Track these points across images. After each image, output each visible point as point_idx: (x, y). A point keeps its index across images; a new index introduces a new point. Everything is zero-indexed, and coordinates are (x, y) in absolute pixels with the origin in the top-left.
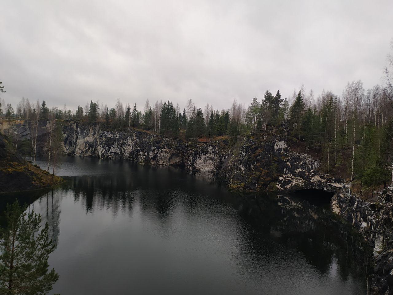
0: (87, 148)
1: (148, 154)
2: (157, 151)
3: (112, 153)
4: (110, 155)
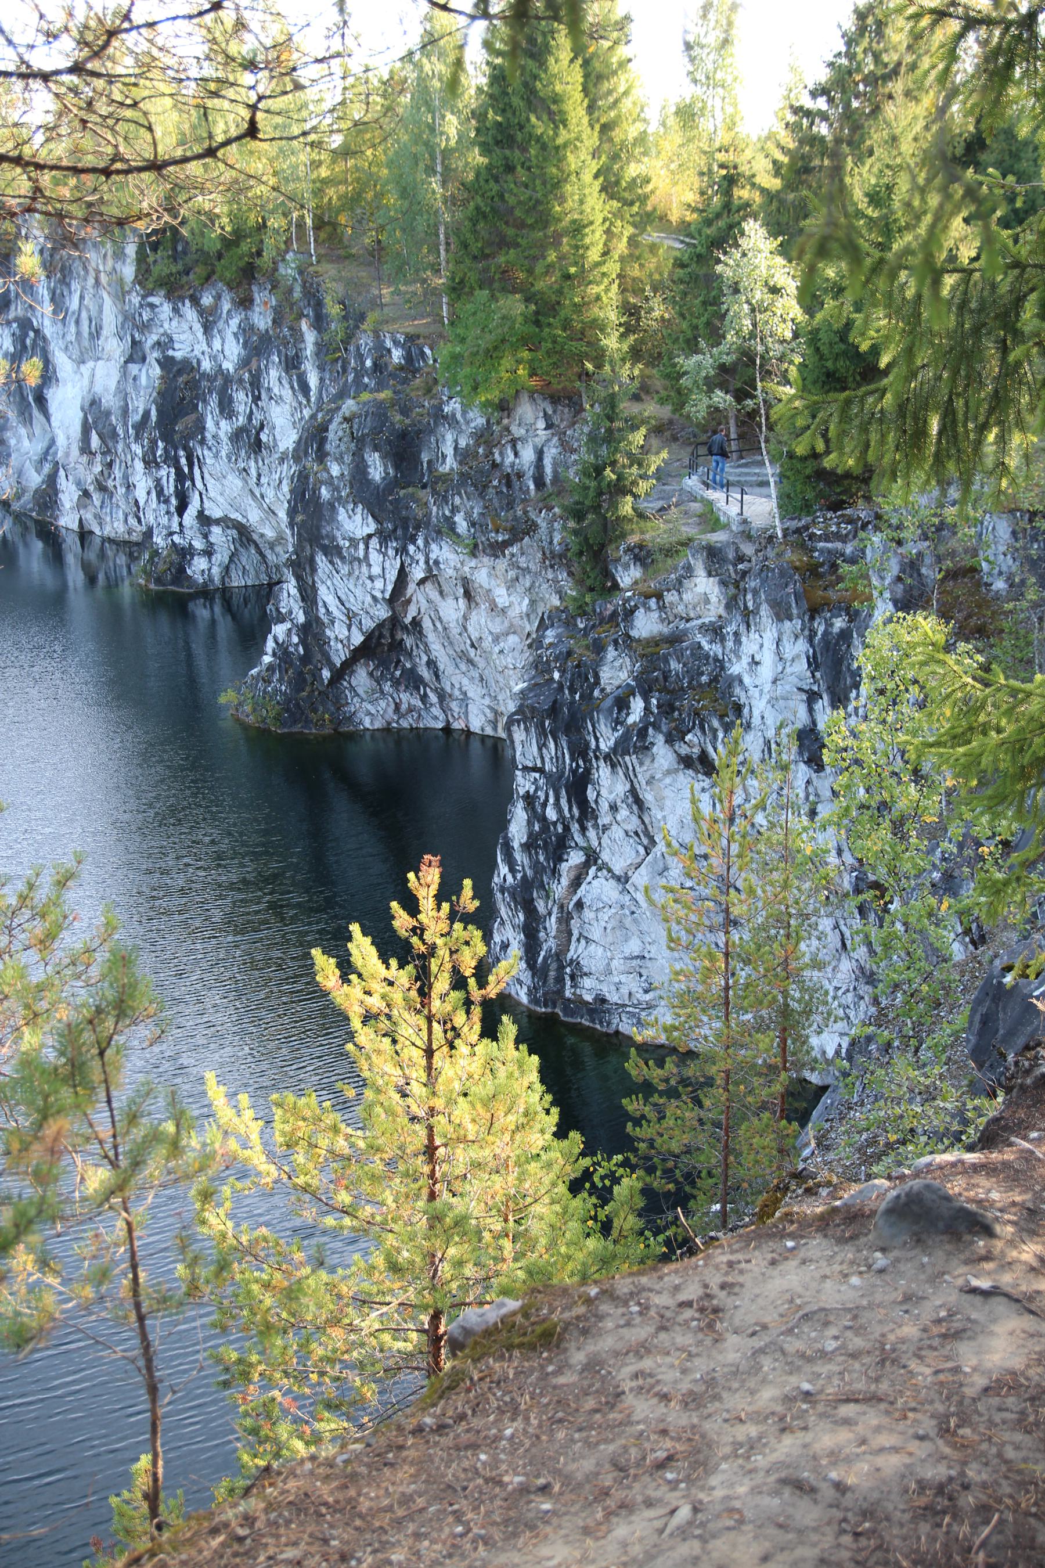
0: (98, 468)
1: (308, 596)
2: (392, 575)
3: (216, 530)
4: (198, 544)
